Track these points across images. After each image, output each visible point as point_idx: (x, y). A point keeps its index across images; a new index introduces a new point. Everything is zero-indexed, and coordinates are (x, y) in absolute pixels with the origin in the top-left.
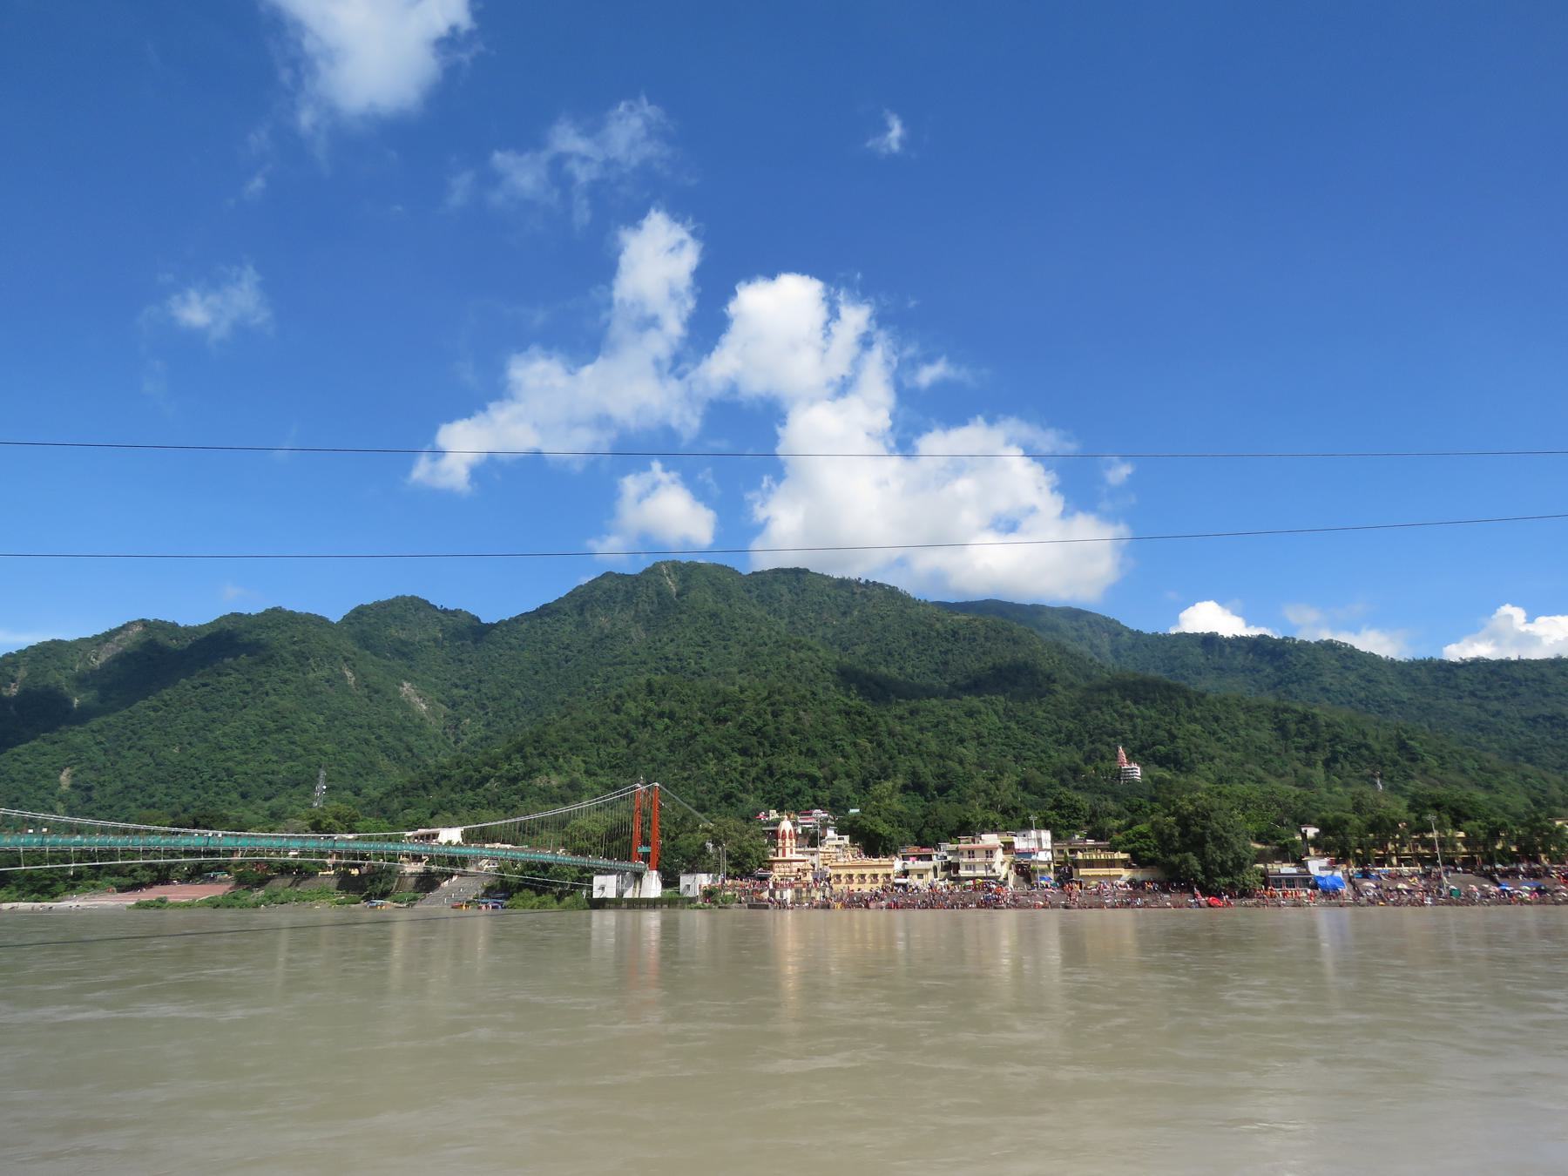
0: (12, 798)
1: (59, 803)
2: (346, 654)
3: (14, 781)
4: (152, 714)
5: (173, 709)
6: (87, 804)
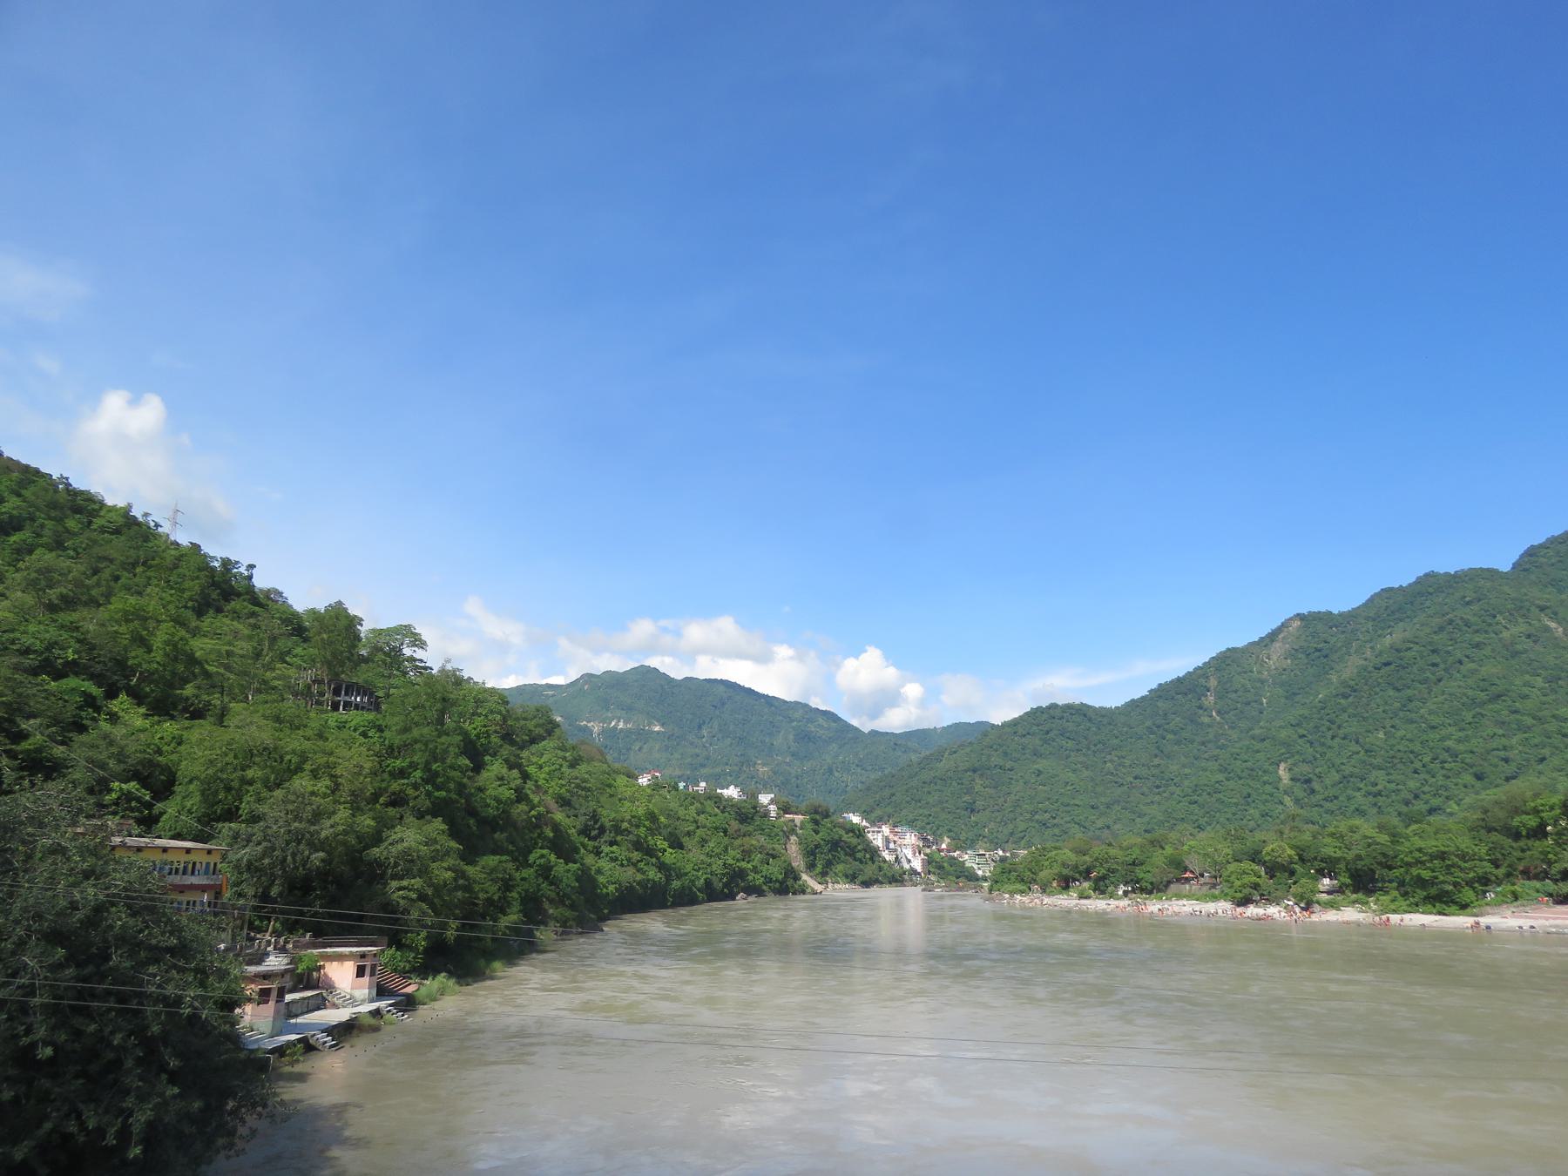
0: (1245, 793)
1: (1286, 797)
2: (1537, 602)
3: (1240, 778)
4: (1342, 701)
5: (1362, 694)
6: (1312, 796)
